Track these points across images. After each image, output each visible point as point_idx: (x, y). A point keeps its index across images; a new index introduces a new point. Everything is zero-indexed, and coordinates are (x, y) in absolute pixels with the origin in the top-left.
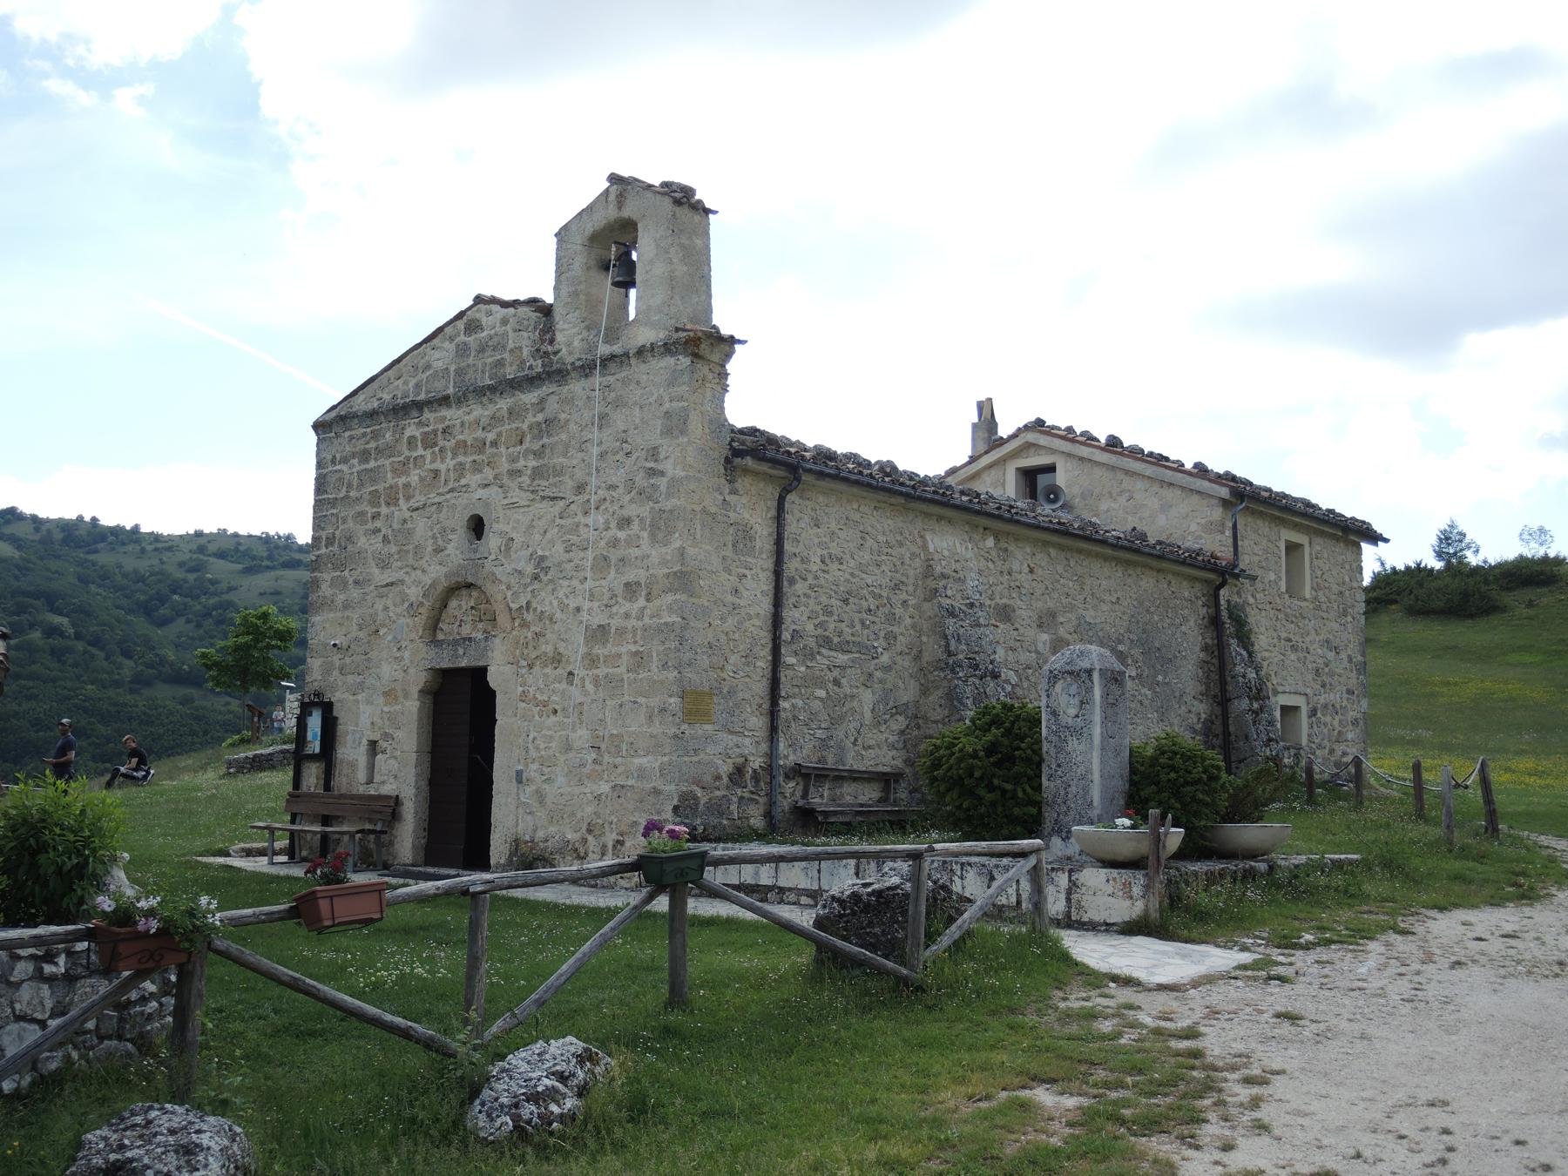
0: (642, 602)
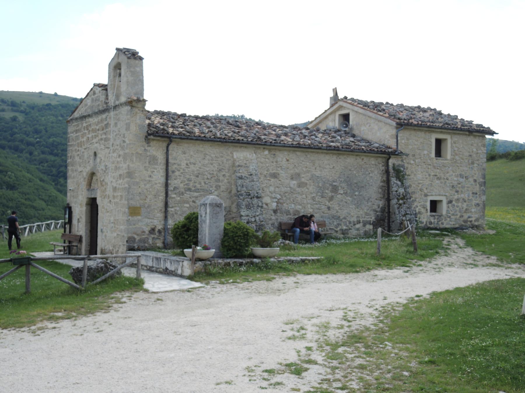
0: (122, 181)
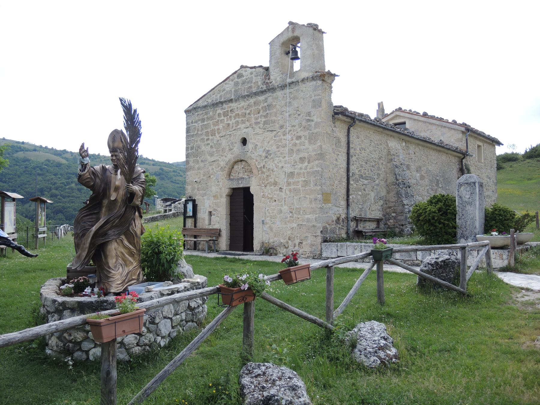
0: (306, 164)
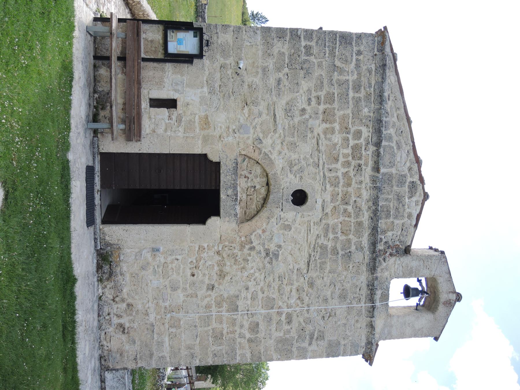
0: (248, 336)
